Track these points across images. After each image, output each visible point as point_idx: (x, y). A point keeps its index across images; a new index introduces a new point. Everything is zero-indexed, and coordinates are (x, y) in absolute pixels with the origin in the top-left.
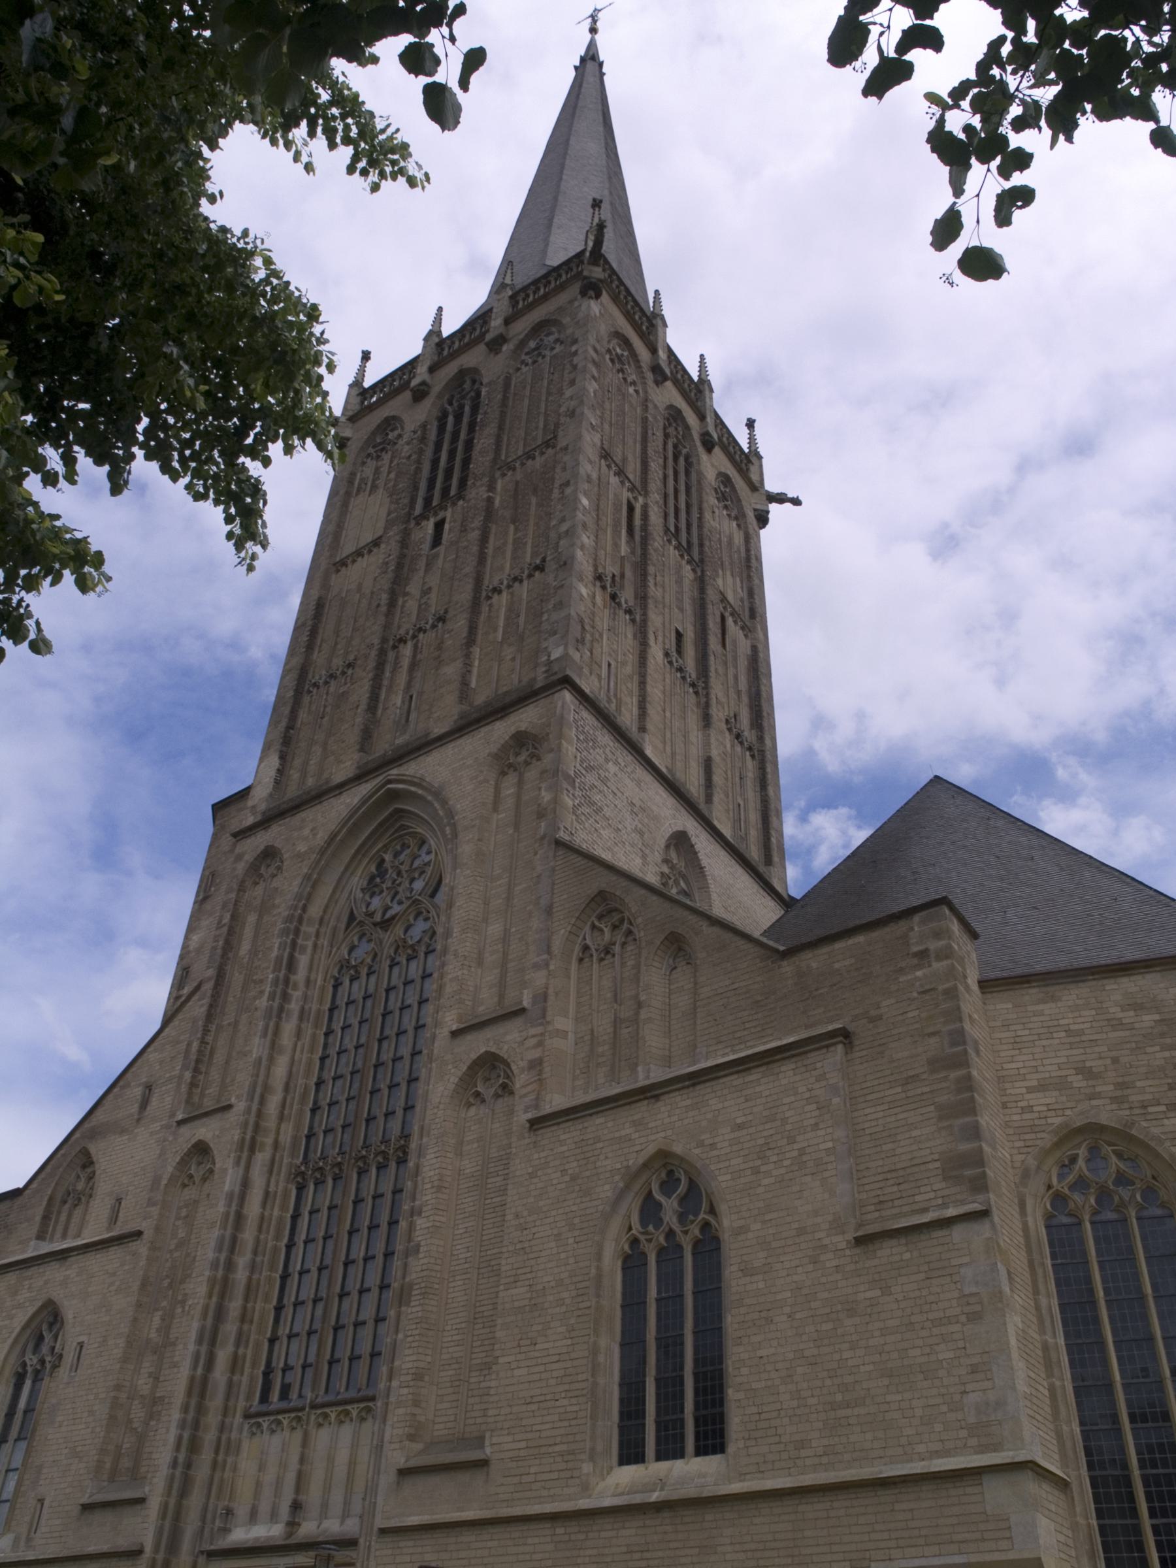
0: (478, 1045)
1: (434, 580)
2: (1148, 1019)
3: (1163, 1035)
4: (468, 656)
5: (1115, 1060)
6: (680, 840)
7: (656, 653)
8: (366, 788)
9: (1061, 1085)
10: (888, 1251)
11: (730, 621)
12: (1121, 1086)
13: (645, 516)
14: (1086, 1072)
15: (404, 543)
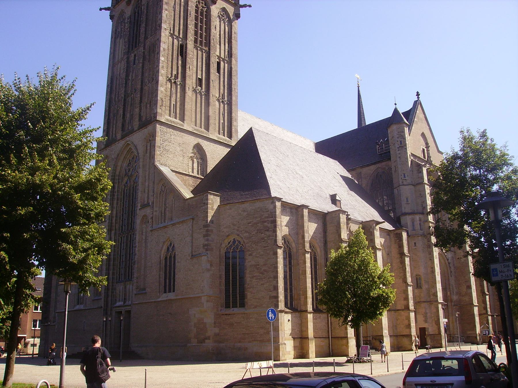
4: (140, 106)
13: (186, 47)
14: (234, 225)
15: (128, 62)
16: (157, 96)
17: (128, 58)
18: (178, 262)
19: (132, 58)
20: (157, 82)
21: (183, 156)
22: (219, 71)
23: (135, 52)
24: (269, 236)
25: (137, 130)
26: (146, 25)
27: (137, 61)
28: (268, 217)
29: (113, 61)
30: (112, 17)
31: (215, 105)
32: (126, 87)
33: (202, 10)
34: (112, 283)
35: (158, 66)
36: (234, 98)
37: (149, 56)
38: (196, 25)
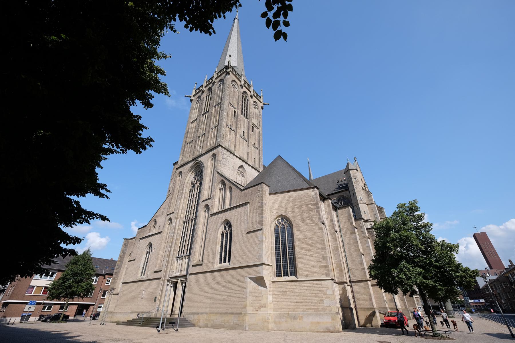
0: (205, 203)
2: (291, 199)
7: (238, 136)
8: (193, 162)
9: (278, 209)
10: (251, 234)
11: (254, 127)
13: (238, 113)
14: (282, 207)
18: (235, 237)
24: (314, 215)
28: (311, 201)
34: (173, 257)
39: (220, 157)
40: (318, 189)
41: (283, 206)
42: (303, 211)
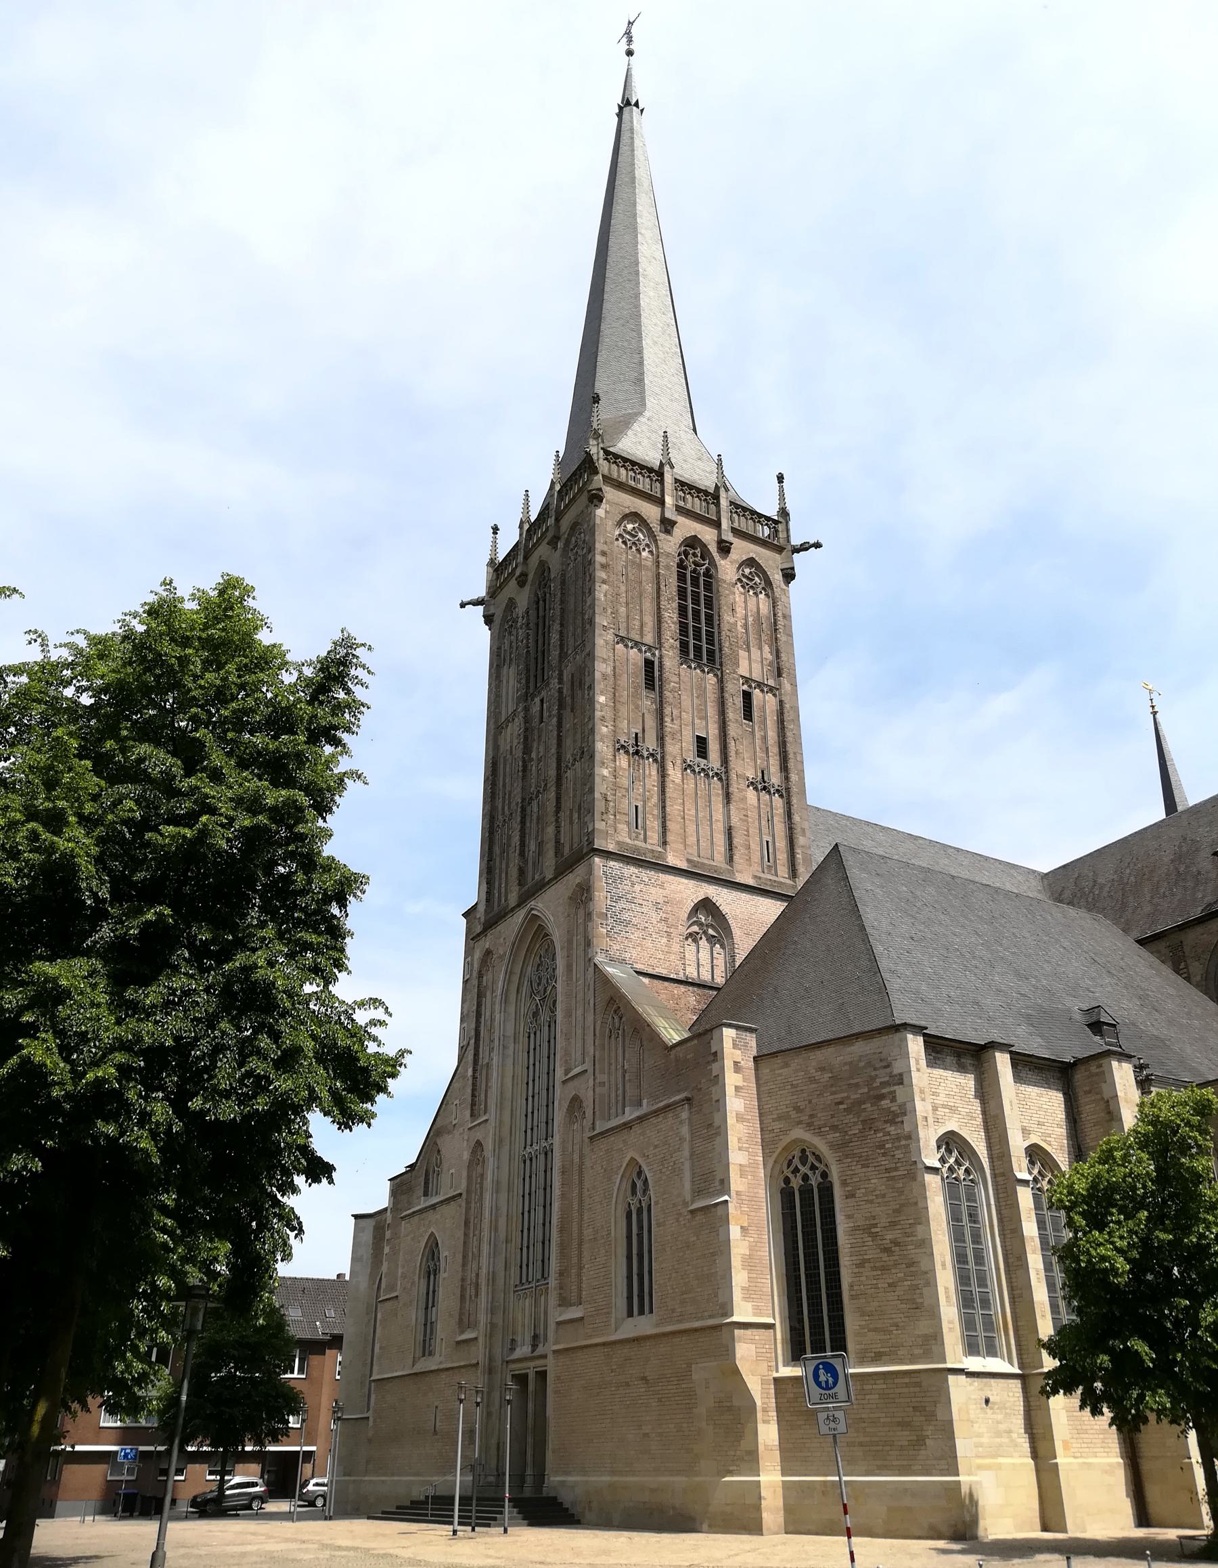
1: (542, 749)
2: (827, 1075)
3: (832, 1086)
5: (810, 1102)
6: (706, 905)
7: (674, 774)
12: (811, 1116)
15: (527, 720)
16: (592, 790)
17: (526, 709)
18: (659, 1225)
19: (535, 709)
20: (592, 757)
21: (669, 934)
22: (748, 715)
23: (543, 693)
25: (551, 880)
26: (562, 625)
27: (545, 714)
29: (496, 722)
30: (488, 620)
31: (744, 799)
32: (524, 777)
33: (694, 571)
35: (592, 718)
36: (794, 777)
37: (573, 698)
38: (682, 610)
39: (601, 897)
40: (918, 1030)
41: (802, 1104)
42: (864, 1122)
